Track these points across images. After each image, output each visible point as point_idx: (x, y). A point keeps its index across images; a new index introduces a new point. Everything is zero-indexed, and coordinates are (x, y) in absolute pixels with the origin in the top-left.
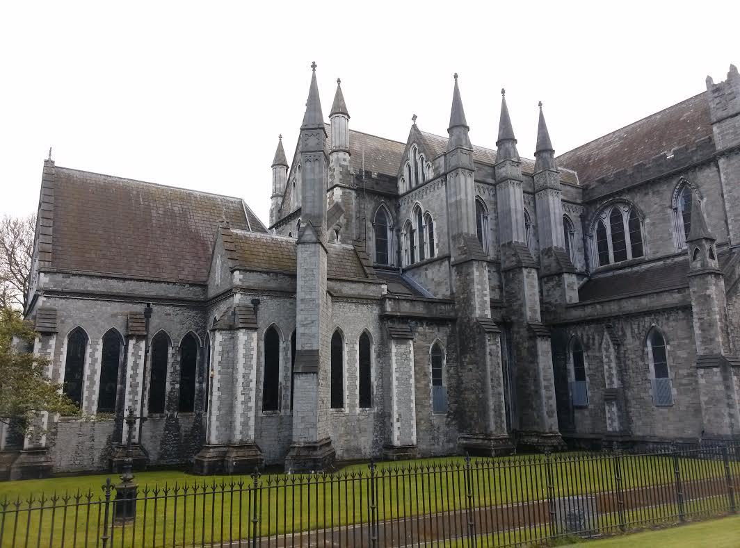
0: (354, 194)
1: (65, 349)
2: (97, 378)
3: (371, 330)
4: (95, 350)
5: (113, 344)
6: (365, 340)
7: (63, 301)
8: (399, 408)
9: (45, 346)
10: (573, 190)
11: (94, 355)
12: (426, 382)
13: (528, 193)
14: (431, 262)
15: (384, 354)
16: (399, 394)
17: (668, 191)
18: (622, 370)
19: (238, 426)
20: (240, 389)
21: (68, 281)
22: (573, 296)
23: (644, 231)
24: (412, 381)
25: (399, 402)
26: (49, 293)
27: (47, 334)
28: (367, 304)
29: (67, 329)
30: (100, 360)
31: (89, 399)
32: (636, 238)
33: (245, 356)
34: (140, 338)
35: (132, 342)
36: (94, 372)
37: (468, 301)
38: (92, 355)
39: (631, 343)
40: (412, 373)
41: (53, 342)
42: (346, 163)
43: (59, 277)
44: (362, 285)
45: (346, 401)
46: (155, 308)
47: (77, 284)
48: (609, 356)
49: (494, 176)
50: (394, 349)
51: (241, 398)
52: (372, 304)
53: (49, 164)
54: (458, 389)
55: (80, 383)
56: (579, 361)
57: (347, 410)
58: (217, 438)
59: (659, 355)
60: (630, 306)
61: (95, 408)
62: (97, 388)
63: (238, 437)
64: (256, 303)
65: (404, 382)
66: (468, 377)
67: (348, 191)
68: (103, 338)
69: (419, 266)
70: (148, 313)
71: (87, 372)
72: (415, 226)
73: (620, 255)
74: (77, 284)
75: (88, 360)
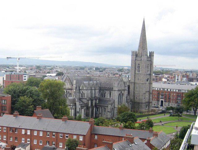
14: (84, 99)
17: (109, 91)
18: (102, 111)
22: (98, 102)
23: (106, 94)
32: (105, 95)
37: (88, 104)
39: (103, 108)
48: (101, 110)
54: (87, 113)
56: (97, 109)
59: (105, 110)
60: (103, 105)
66: (88, 112)
69: (82, 98)
72: (82, 93)
73: (103, 97)
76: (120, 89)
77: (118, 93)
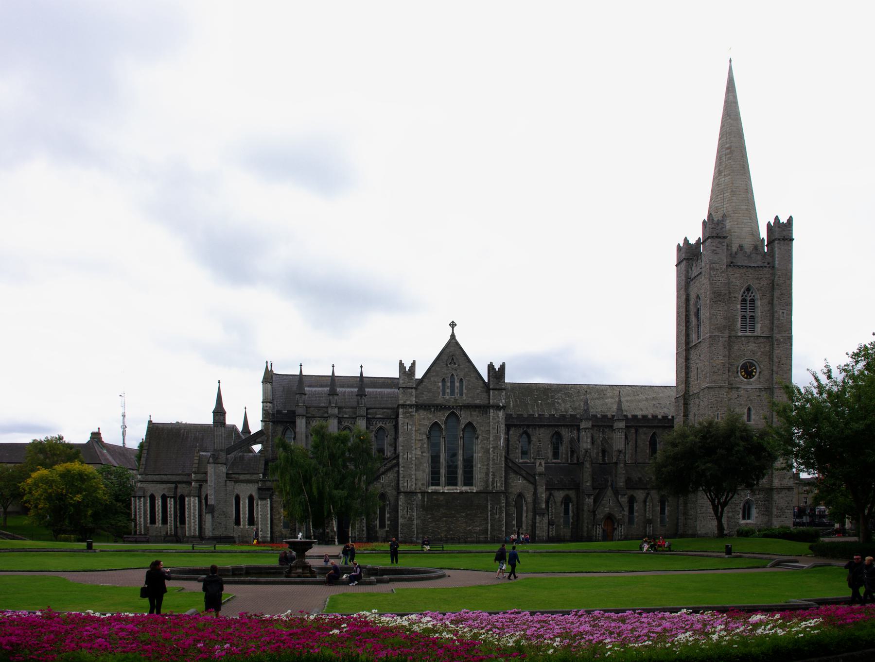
0: (271, 424)
1: (148, 501)
2: (160, 511)
3: (254, 494)
4: (158, 501)
5: (164, 498)
6: (251, 499)
7: (145, 484)
8: (262, 526)
9: (140, 501)
10: (389, 411)
11: (159, 503)
12: (279, 516)
13: (353, 418)
15: (257, 505)
16: (261, 521)
19: (192, 531)
20: (192, 518)
21: (147, 477)
24: (269, 516)
25: (262, 524)
26: (141, 482)
27: (140, 497)
28: (252, 483)
29: (149, 494)
30: (161, 505)
31: (158, 519)
33: (193, 506)
34: (171, 497)
35: (168, 499)
36: (159, 510)
38: (158, 503)
40: (269, 512)
41: (142, 499)
42: (267, 408)
43: (144, 476)
44: (249, 475)
45: (242, 523)
46: (179, 485)
47: (150, 478)
49: (327, 412)
50: (259, 503)
51: (192, 521)
52: (254, 483)
53: (150, 422)
55: (155, 513)
57: (242, 527)
58: (188, 534)
61: (160, 522)
62: (160, 515)
63: (192, 534)
64: (201, 486)
65: (264, 516)
67: (268, 423)
68: (161, 497)
70: (176, 487)
71: (157, 510)
74: (150, 478)
75: (157, 505)
76: (440, 400)
77: (428, 423)
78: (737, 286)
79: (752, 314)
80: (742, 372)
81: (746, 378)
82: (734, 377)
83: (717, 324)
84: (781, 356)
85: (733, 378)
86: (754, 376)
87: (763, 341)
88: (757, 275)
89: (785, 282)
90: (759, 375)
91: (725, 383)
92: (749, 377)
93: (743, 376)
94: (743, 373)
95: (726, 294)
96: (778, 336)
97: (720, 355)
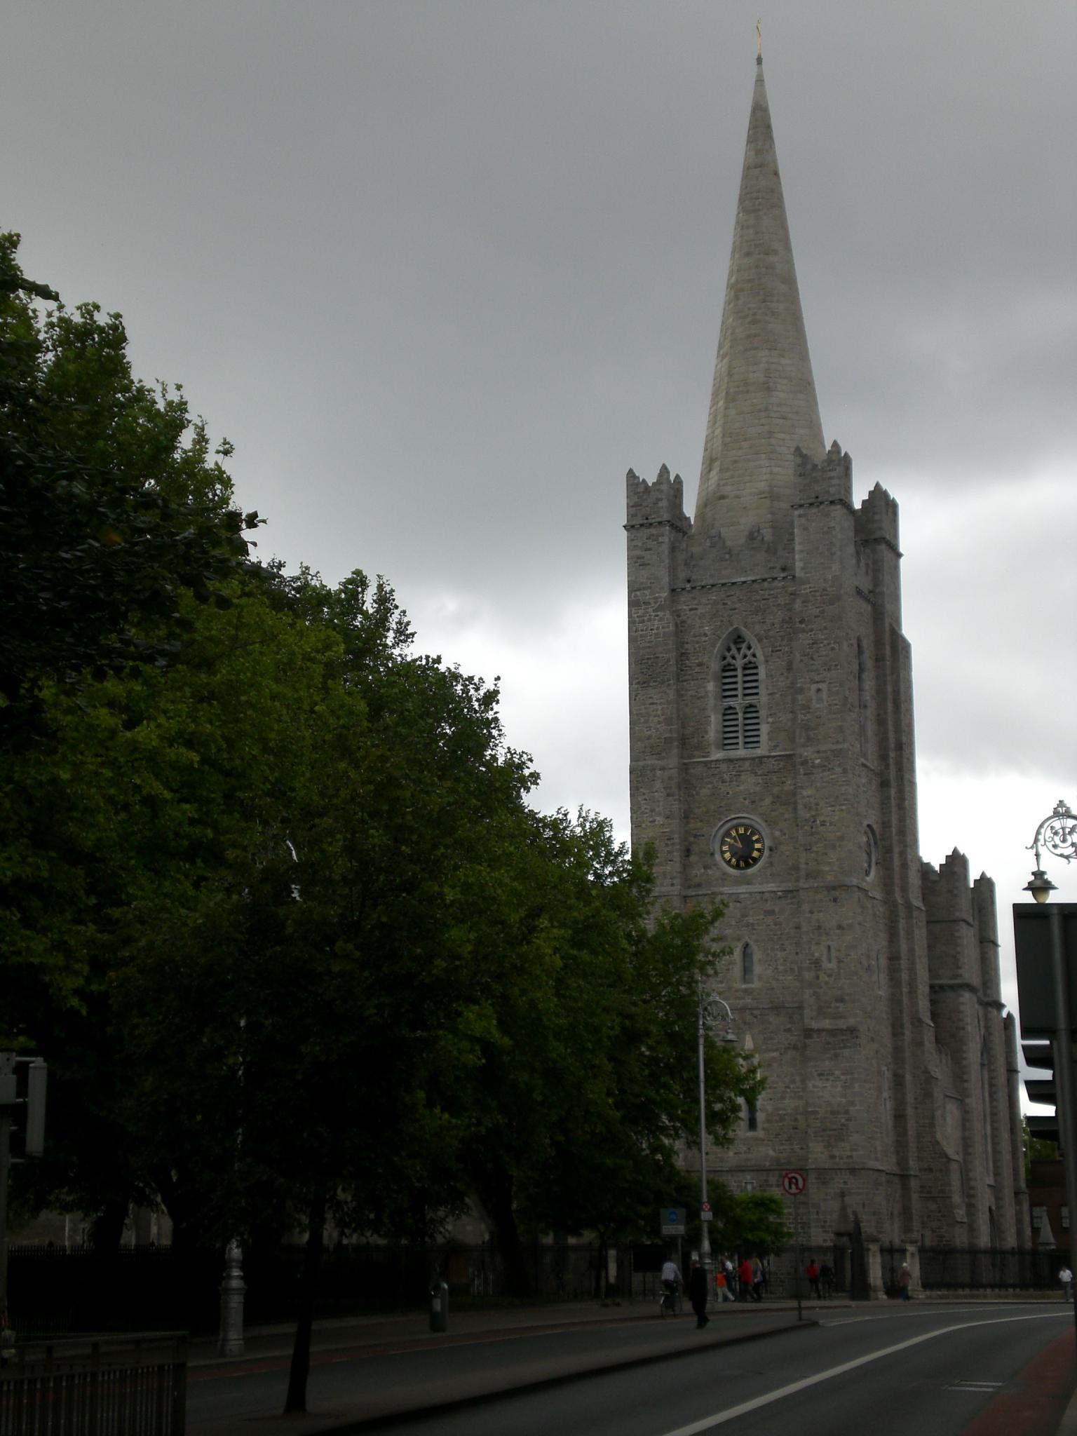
78: (705, 635)
79: (750, 700)
80: (758, 850)
81: (737, 866)
82: (705, 867)
83: (649, 738)
84: (817, 804)
85: (703, 871)
86: (755, 860)
87: (776, 768)
88: (756, 601)
89: (822, 612)
90: (770, 856)
91: (673, 885)
92: (742, 864)
93: (729, 862)
94: (727, 855)
95: (669, 660)
96: (807, 753)
97: (660, 814)
